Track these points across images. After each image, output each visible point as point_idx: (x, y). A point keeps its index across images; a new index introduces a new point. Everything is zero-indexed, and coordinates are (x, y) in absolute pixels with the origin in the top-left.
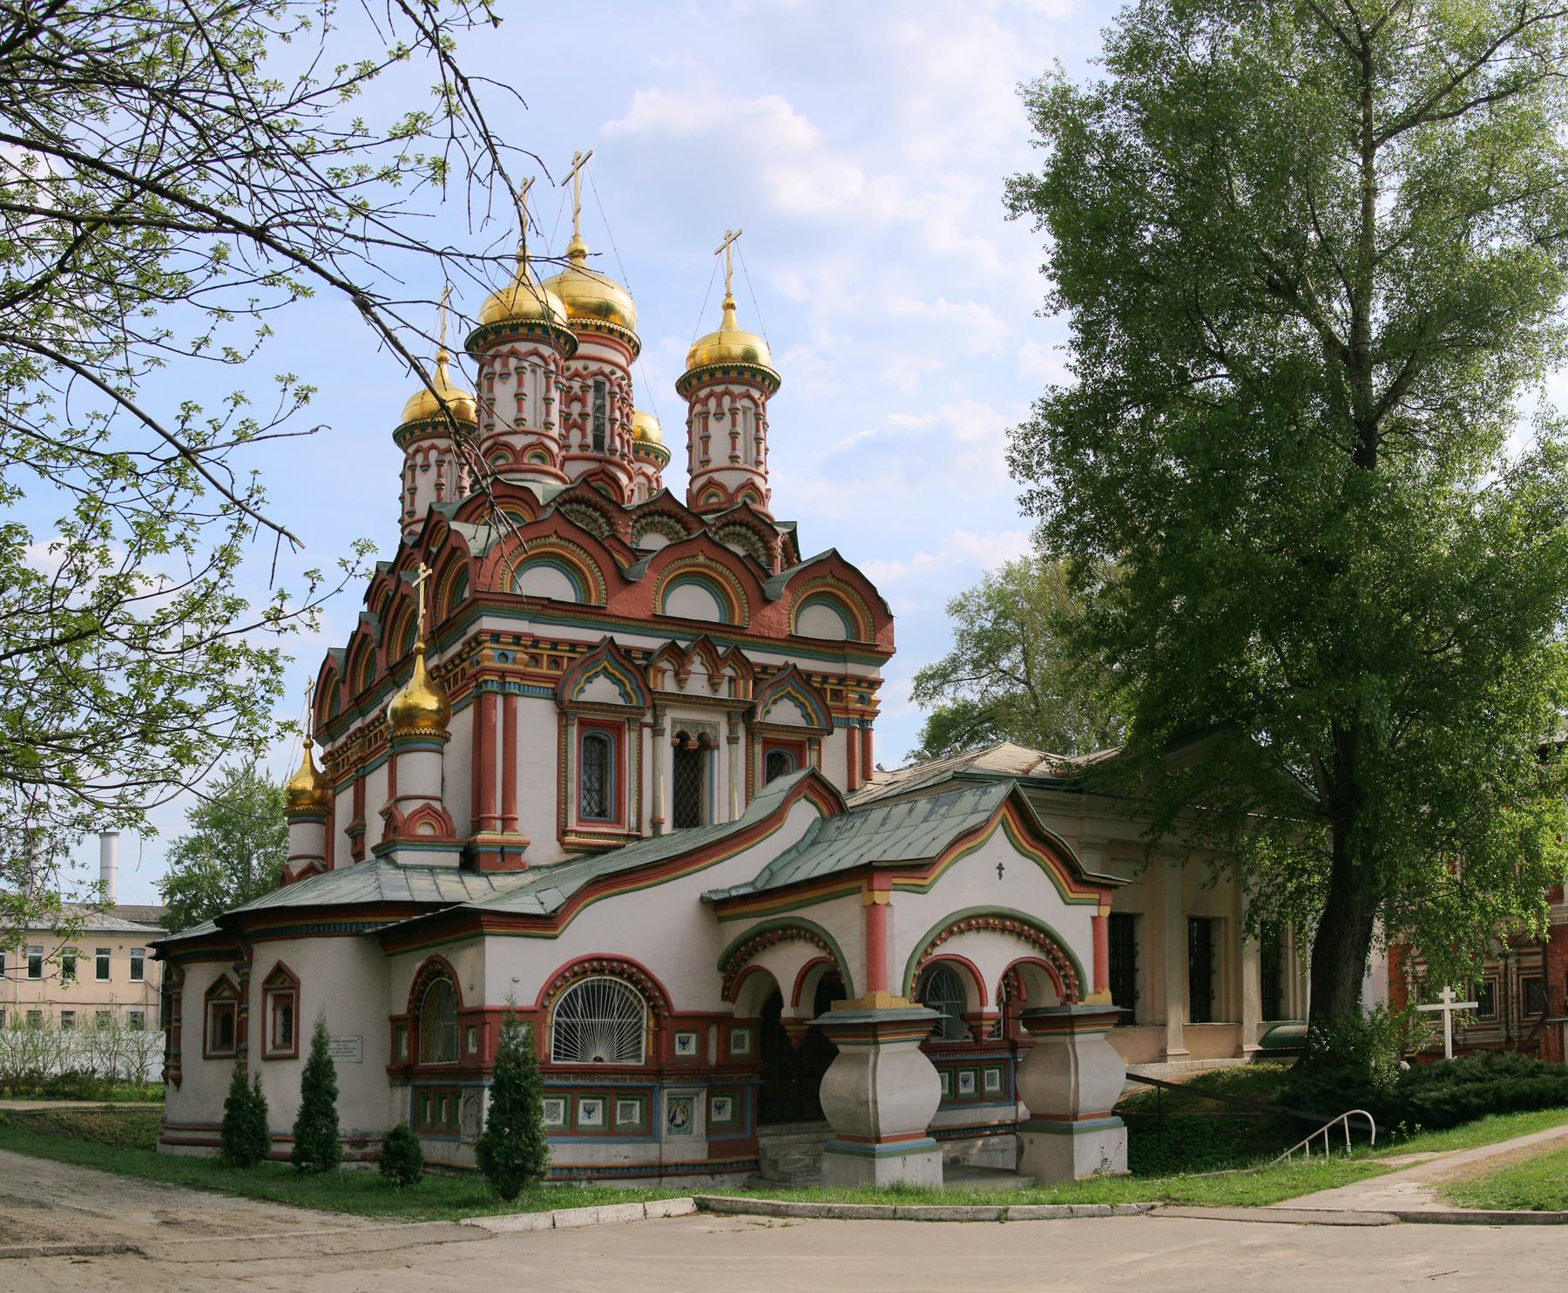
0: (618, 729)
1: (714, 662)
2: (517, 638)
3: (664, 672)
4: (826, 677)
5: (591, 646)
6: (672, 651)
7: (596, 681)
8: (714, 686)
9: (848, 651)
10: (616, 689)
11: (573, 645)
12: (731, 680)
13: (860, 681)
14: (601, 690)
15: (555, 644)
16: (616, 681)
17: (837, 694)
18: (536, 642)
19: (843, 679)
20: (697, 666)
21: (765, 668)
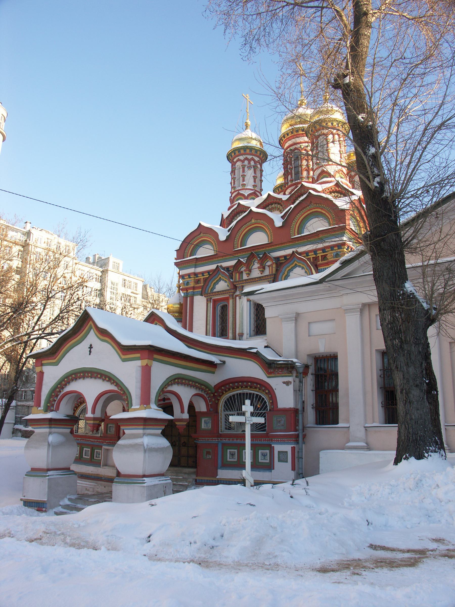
0: (227, 299)
1: (262, 261)
2: (189, 275)
3: (242, 272)
4: (315, 251)
5: (214, 271)
6: (239, 263)
7: (220, 283)
8: (262, 272)
9: (321, 236)
10: (226, 284)
11: (208, 272)
12: (269, 266)
13: (332, 247)
14: (222, 286)
15: (203, 273)
16: (226, 282)
17: (324, 257)
18: (196, 274)
19: (323, 250)
20: (256, 265)
21: (285, 257)
